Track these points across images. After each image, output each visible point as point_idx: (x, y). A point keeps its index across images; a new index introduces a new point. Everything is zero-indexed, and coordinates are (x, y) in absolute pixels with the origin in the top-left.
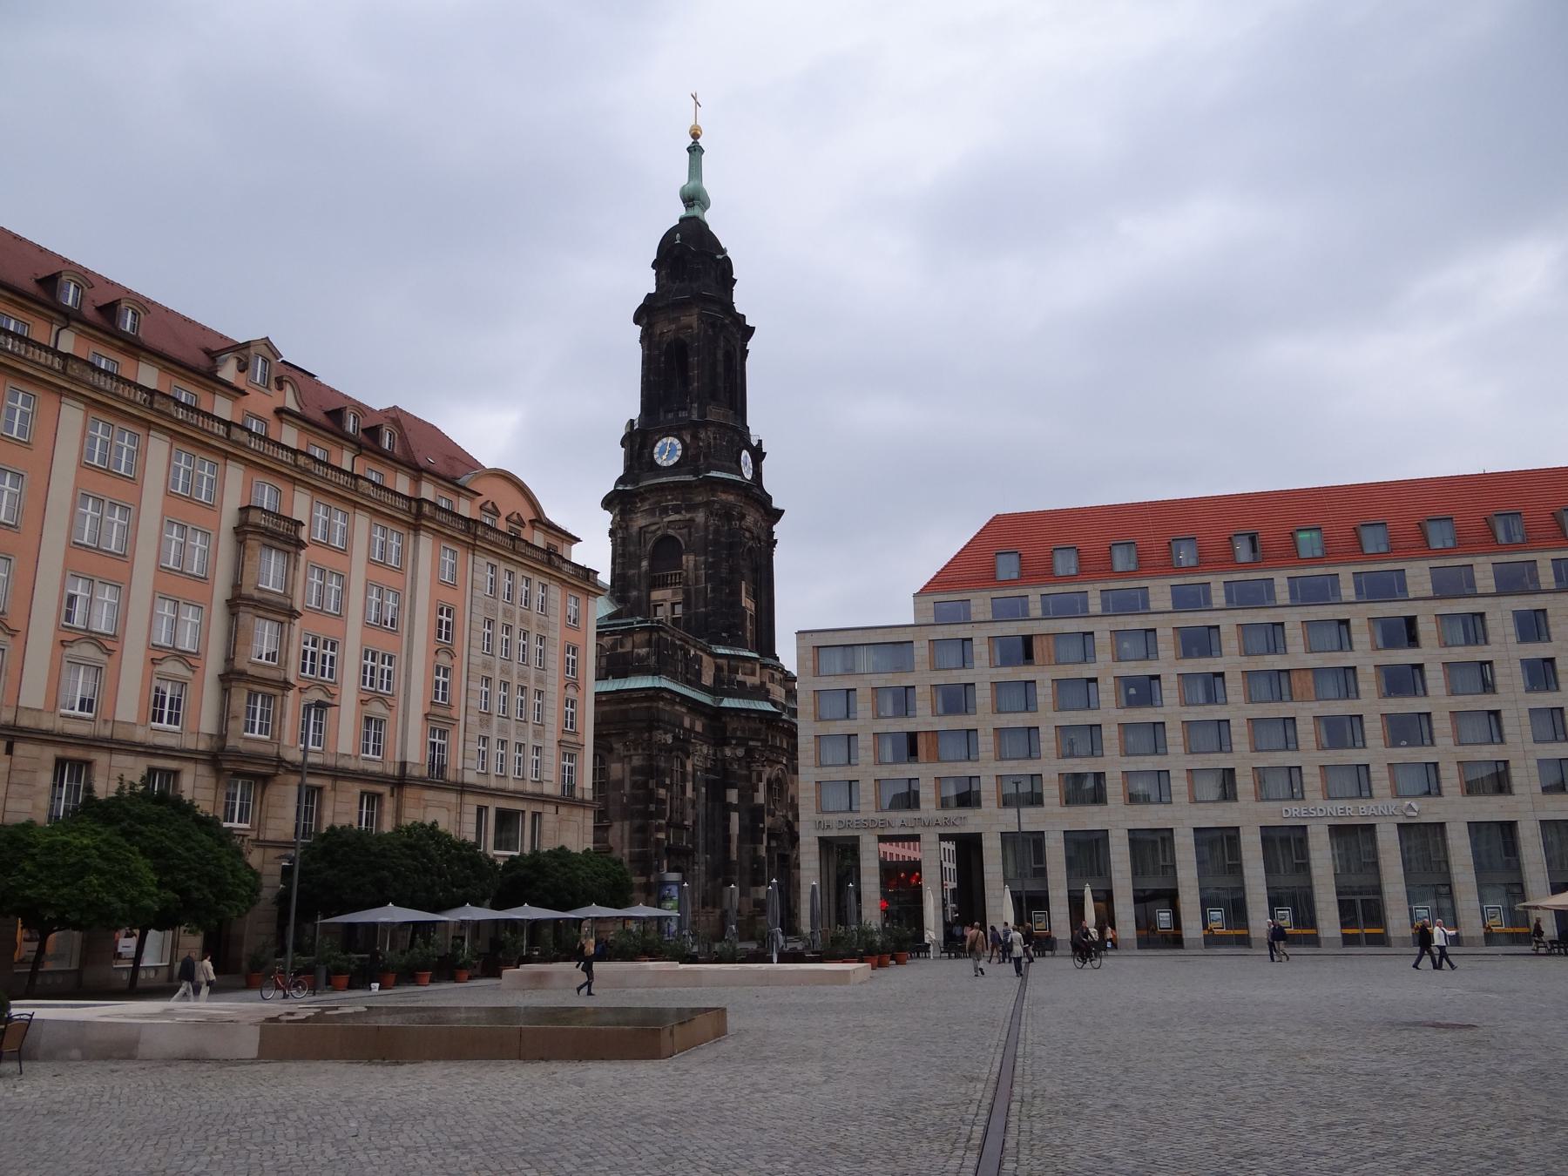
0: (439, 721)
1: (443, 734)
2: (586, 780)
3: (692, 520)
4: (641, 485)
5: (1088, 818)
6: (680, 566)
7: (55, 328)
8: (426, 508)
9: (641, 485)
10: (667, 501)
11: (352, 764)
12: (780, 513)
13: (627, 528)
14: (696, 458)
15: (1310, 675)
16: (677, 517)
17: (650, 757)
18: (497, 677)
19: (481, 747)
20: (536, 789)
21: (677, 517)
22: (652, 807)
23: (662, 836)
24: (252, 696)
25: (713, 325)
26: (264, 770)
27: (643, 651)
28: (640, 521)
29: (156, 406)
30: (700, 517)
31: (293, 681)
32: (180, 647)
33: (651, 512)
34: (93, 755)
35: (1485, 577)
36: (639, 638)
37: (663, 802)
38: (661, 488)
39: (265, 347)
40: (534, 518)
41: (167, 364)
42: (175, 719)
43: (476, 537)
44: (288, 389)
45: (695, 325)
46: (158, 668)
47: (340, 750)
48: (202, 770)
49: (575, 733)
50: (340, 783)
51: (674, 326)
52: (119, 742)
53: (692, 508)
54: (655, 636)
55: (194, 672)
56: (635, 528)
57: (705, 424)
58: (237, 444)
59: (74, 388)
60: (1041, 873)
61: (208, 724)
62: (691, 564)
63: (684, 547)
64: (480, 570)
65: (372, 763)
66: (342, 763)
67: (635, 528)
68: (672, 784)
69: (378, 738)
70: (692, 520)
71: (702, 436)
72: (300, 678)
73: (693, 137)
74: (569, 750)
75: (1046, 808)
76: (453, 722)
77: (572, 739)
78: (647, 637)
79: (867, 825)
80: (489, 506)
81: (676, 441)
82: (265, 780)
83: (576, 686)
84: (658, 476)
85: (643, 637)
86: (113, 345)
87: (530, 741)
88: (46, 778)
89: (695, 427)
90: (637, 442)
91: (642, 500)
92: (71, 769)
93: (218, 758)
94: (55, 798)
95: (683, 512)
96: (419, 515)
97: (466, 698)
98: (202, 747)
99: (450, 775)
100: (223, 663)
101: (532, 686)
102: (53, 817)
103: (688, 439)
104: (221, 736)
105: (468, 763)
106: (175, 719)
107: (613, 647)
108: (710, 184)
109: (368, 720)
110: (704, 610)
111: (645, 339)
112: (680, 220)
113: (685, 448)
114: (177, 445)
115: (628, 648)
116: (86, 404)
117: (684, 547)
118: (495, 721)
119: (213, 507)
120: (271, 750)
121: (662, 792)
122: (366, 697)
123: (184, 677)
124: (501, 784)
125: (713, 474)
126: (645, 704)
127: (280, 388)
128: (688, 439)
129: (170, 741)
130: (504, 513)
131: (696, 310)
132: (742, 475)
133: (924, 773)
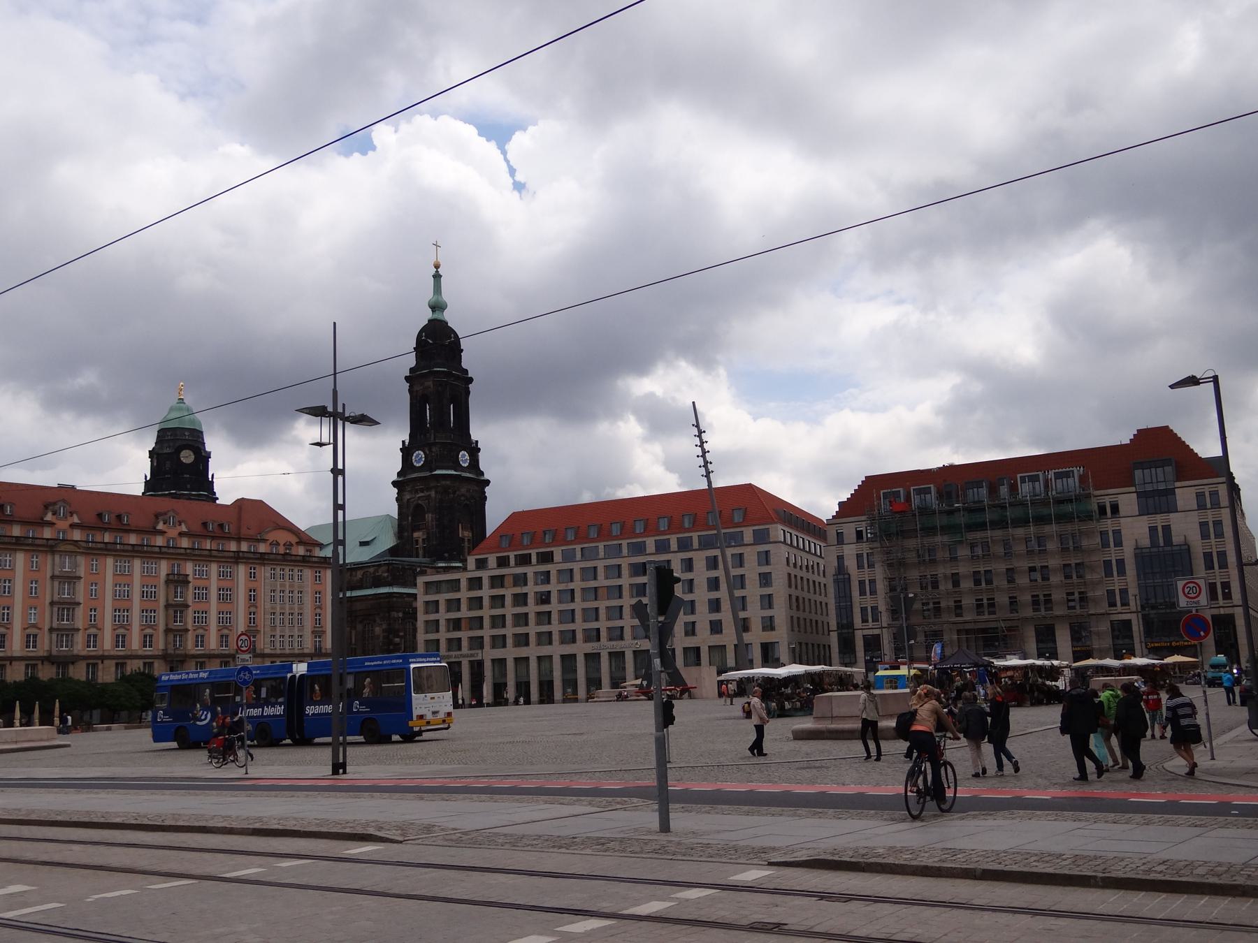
1: (254, 637)
2: (328, 643)
3: (429, 495)
5: (545, 650)
8: (241, 554)
10: (418, 486)
11: (216, 652)
12: (487, 482)
13: (401, 500)
15: (606, 588)
16: (422, 494)
18: (278, 611)
19: (272, 639)
20: (301, 652)
21: (422, 494)
22: (391, 647)
24: (175, 636)
26: (181, 659)
27: (386, 574)
28: (407, 496)
30: (433, 493)
31: (190, 628)
33: (410, 492)
34: (127, 661)
35: (674, 545)
36: (384, 568)
37: (398, 644)
40: (298, 540)
42: (151, 646)
44: (183, 525)
45: (432, 386)
47: (211, 648)
48: (160, 661)
49: (322, 627)
50: (211, 660)
51: (422, 388)
52: (133, 656)
53: (429, 489)
56: (405, 500)
57: (435, 444)
60: (505, 675)
61: (161, 646)
62: (430, 519)
63: (426, 509)
64: (264, 572)
66: (212, 652)
67: (405, 500)
68: (405, 635)
69: (227, 641)
70: (429, 495)
71: (434, 450)
72: (193, 626)
73: (435, 267)
74: (318, 633)
75: (508, 648)
76: (258, 631)
77: (320, 629)
78: (387, 567)
80: (275, 542)
81: (422, 453)
83: (320, 607)
85: (386, 568)
87: (296, 633)
88: (113, 669)
89: (430, 445)
90: (407, 451)
91: (408, 485)
92: (120, 665)
93: (165, 657)
94: (117, 674)
95: (425, 492)
97: (263, 621)
98: (160, 654)
101: (296, 611)
102: (116, 679)
103: (428, 452)
104: (166, 649)
105: (266, 646)
106: (151, 646)
107: (374, 573)
108: (446, 296)
109: (222, 636)
110: (434, 543)
112: (429, 321)
115: (380, 573)
117: (426, 509)
118: (278, 629)
119: (157, 577)
121: (397, 640)
122: (220, 628)
124: (283, 652)
126: (387, 600)
127: (180, 525)
128: (428, 452)
129: (150, 653)
130: (282, 544)
132: (457, 465)
133: (464, 635)
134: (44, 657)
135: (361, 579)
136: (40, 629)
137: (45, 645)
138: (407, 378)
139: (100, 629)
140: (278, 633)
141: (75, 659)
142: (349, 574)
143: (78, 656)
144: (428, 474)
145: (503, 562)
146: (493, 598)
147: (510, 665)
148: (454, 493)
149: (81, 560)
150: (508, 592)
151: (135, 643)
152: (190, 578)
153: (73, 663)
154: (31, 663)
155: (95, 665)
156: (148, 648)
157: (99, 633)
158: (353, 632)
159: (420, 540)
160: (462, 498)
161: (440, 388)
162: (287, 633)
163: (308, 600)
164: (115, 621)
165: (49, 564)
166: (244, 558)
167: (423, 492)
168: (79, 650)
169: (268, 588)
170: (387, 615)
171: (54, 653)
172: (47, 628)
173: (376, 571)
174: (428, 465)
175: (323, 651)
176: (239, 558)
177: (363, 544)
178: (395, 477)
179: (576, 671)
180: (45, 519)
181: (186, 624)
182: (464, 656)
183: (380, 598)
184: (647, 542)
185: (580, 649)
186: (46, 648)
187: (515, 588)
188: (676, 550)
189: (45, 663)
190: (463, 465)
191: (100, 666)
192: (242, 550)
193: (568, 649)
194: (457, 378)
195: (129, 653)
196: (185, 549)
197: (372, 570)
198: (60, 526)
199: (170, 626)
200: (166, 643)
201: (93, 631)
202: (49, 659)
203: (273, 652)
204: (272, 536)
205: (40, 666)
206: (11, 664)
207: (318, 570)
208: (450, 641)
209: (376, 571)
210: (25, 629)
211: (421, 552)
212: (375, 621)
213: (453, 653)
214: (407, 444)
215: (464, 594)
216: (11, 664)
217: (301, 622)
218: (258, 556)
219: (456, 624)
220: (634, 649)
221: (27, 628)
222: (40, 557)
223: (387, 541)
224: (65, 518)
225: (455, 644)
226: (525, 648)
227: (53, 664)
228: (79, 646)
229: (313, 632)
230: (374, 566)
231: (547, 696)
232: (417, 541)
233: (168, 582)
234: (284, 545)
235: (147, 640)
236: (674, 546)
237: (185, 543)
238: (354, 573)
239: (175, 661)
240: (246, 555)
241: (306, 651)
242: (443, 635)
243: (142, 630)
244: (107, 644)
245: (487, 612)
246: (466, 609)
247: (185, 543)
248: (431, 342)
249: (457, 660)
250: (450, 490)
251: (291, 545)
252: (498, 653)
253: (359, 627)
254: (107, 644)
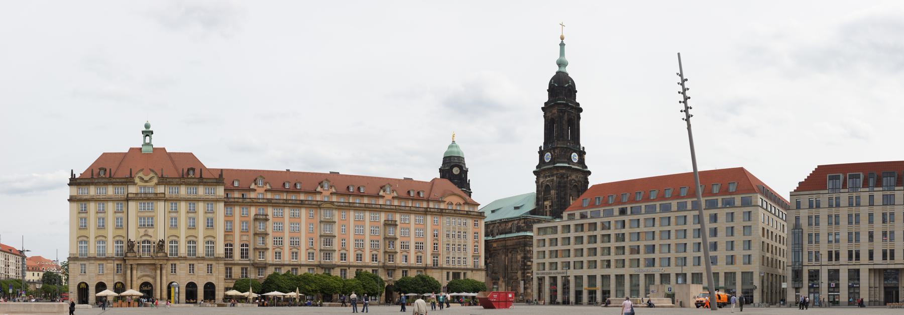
0: (435, 255)
1: (437, 257)
3: (553, 179)
4: (542, 168)
6: (550, 194)
9: (542, 168)
11: (414, 265)
14: (555, 158)
16: (549, 179)
17: (525, 254)
20: (465, 267)
21: (549, 179)
22: (526, 267)
23: (530, 275)
24: (389, 256)
25: (562, 112)
27: (523, 225)
28: (541, 180)
30: (555, 178)
33: (543, 177)
34: (362, 268)
36: (523, 221)
38: (544, 170)
40: (464, 202)
43: (443, 212)
47: (411, 263)
48: (382, 269)
53: (553, 175)
54: (526, 220)
56: (540, 183)
61: (382, 261)
64: (445, 220)
65: (420, 265)
66: (412, 265)
67: (540, 183)
70: (553, 179)
71: (556, 152)
74: (476, 257)
79: (547, 274)
82: (394, 270)
84: (545, 166)
87: (462, 256)
90: (542, 153)
91: (542, 173)
96: (427, 211)
97: (442, 249)
99: (439, 266)
104: (384, 263)
107: (517, 224)
108: (568, 57)
110: (555, 207)
111: (545, 116)
113: (552, 156)
118: (451, 253)
120: (393, 265)
125: (558, 165)
130: (454, 203)
131: (556, 108)
132: (570, 160)
135: (511, 228)
136: (315, 250)
137: (318, 259)
138: (543, 108)
139: (347, 251)
140: (451, 256)
141: (333, 267)
142: (504, 225)
143: (335, 265)
144: (552, 166)
145: (583, 216)
146: (576, 238)
147: (585, 280)
148: (567, 177)
150: (585, 235)
151: (367, 259)
152: (398, 223)
154: (311, 267)
155: (345, 270)
156: (359, 262)
157: (299, 251)
158: (507, 258)
159: (548, 206)
160: (573, 181)
161: (561, 114)
162: (457, 256)
163: (470, 237)
164: (371, 247)
165: (324, 214)
166: (430, 211)
167: (549, 177)
169: (445, 230)
170: (523, 248)
171: (322, 262)
173: (518, 223)
174: (553, 161)
175: (479, 267)
176: (427, 211)
177: (516, 208)
178: (535, 169)
179: (624, 285)
181: (395, 249)
182: (559, 273)
183: (520, 239)
184: (672, 204)
185: (627, 271)
186: (318, 260)
187: (589, 232)
188: (691, 209)
190: (574, 161)
191: (348, 271)
192: (430, 207)
193: (620, 271)
194: (572, 108)
195: (364, 264)
196: (396, 206)
197: (516, 222)
198: (325, 195)
199: (387, 250)
200: (385, 260)
201: (343, 251)
202: (320, 266)
203: (448, 267)
204: (448, 199)
207: (476, 220)
208: (551, 264)
209: (518, 223)
210: (307, 250)
211: (548, 213)
212: (517, 252)
213: (553, 271)
214: (542, 149)
215: (560, 235)
216: (300, 268)
217: (465, 249)
218: (440, 211)
219: (555, 254)
220: (661, 273)
223: (531, 206)
225: (554, 265)
226: (594, 270)
227: (322, 268)
228: (336, 259)
229: (473, 256)
230: (517, 220)
231: (592, 301)
232: (546, 207)
234: (456, 205)
235: (374, 258)
236: (689, 206)
237: (396, 203)
238: (507, 224)
239: (390, 270)
240: (432, 210)
241: (468, 267)
242: (547, 260)
243: (371, 252)
244: (351, 259)
245: (573, 247)
246: (560, 245)
247: (396, 203)
248: (556, 85)
249: (554, 275)
250: (565, 176)
251: (460, 205)
252: (578, 272)
253: (510, 255)
254: (351, 259)
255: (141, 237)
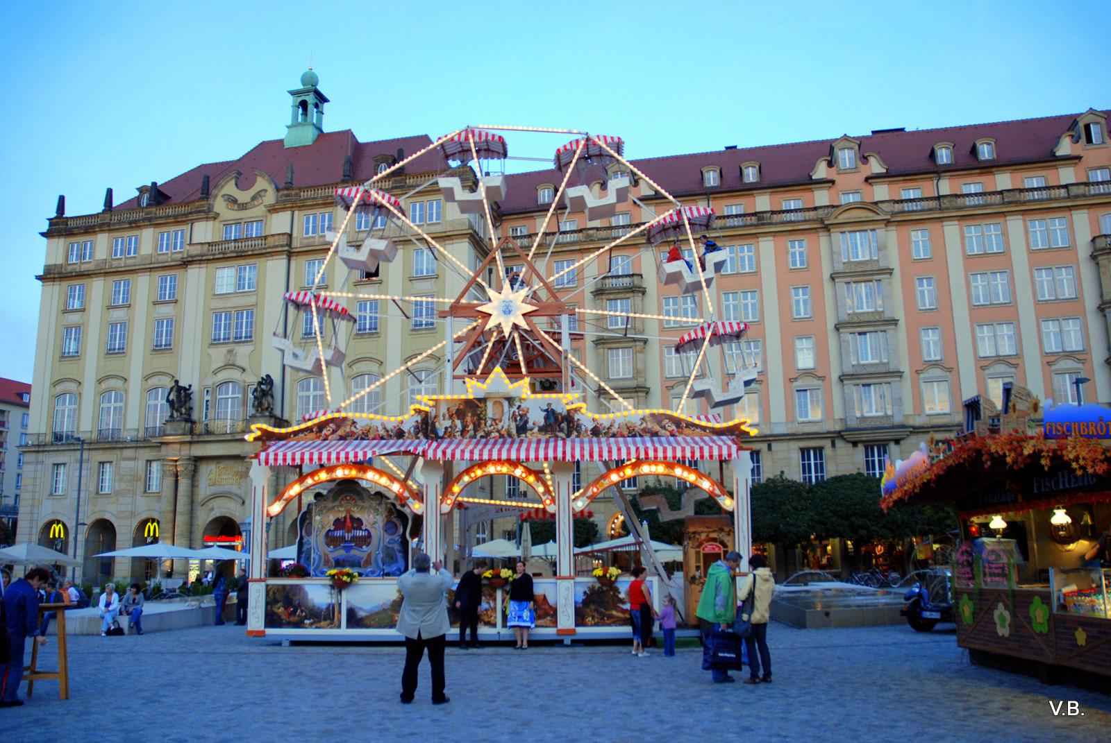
7: (935, 182)
29: (1006, 200)
32: (1068, 350)
39: (1091, 116)
41: (1013, 168)
46: (1053, 367)
55: (1083, 363)
58: (1077, 197)
59: (946, 215)
86: (974, 174)
100: (1107, 351)
114: (1027, 218)
116: (958, 220)
119: (1071, 248)
123: (1076, 369)
134: (835, 432)
139: (950, 370)
143: (903, 426)
149: (891, 236)
153: (897, 442)
168: (907, 416)
172: (835, 376)
180: (814, 178)
189: (839, 443)
205: (828, 451)
206: (770, 448)
210: (791, 380)
221: (796, 379)
222: (805, 243)
224: (855, 170)
227: (855, 444)
233: (1093, 257)
255: (215, 373)
